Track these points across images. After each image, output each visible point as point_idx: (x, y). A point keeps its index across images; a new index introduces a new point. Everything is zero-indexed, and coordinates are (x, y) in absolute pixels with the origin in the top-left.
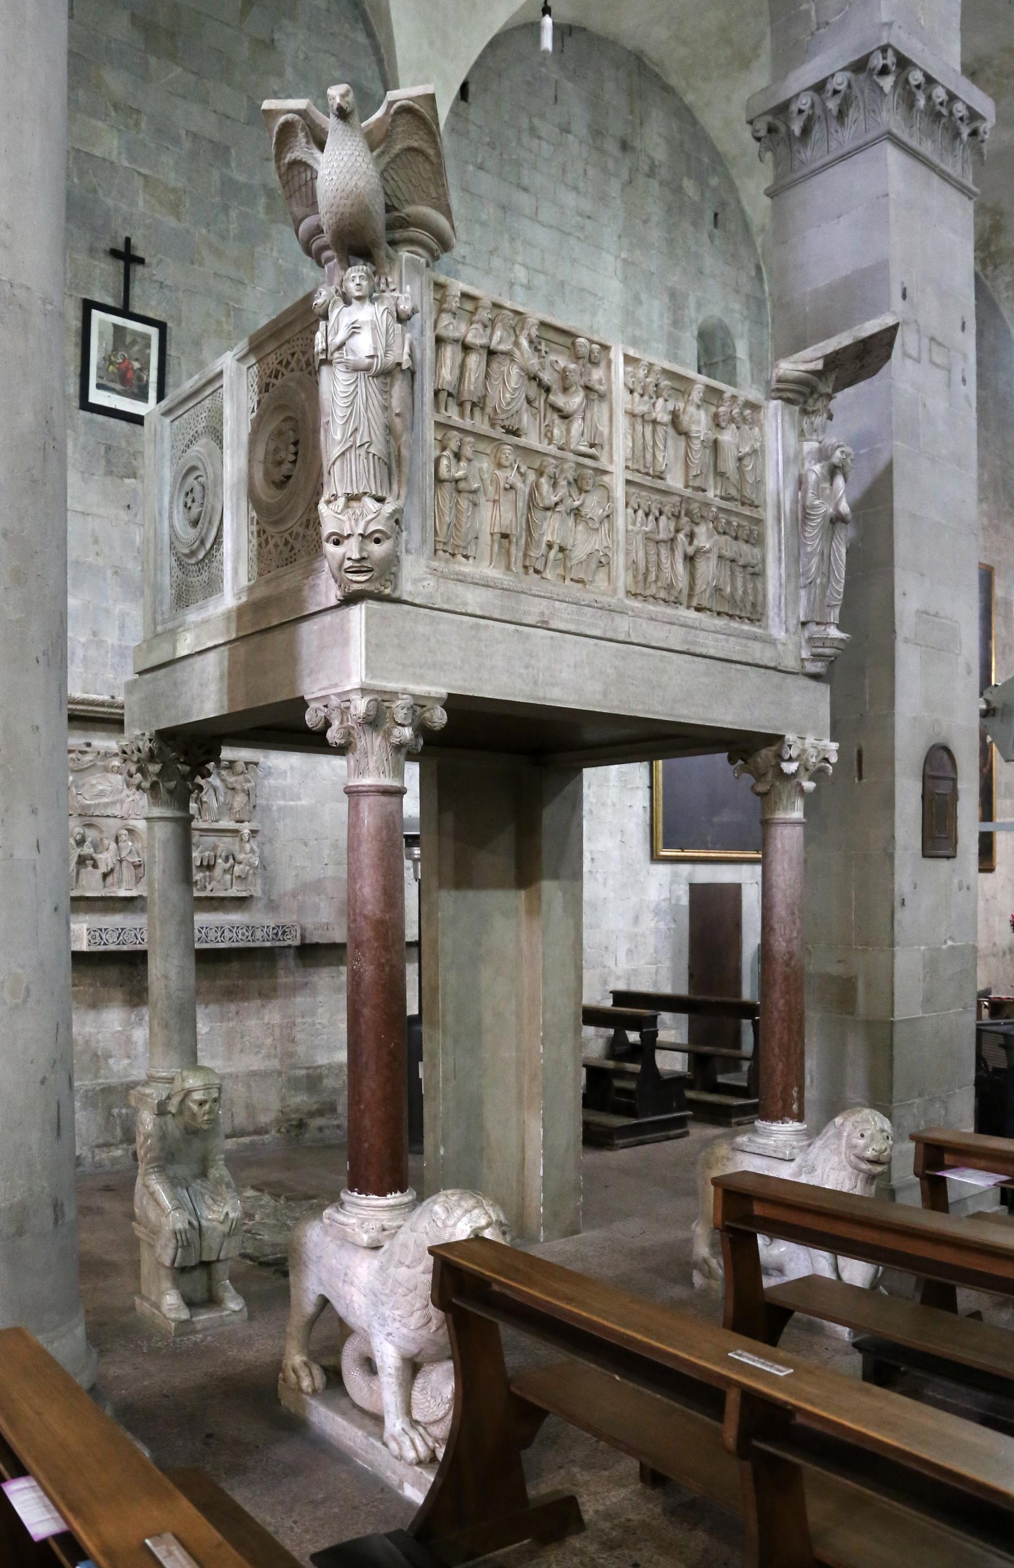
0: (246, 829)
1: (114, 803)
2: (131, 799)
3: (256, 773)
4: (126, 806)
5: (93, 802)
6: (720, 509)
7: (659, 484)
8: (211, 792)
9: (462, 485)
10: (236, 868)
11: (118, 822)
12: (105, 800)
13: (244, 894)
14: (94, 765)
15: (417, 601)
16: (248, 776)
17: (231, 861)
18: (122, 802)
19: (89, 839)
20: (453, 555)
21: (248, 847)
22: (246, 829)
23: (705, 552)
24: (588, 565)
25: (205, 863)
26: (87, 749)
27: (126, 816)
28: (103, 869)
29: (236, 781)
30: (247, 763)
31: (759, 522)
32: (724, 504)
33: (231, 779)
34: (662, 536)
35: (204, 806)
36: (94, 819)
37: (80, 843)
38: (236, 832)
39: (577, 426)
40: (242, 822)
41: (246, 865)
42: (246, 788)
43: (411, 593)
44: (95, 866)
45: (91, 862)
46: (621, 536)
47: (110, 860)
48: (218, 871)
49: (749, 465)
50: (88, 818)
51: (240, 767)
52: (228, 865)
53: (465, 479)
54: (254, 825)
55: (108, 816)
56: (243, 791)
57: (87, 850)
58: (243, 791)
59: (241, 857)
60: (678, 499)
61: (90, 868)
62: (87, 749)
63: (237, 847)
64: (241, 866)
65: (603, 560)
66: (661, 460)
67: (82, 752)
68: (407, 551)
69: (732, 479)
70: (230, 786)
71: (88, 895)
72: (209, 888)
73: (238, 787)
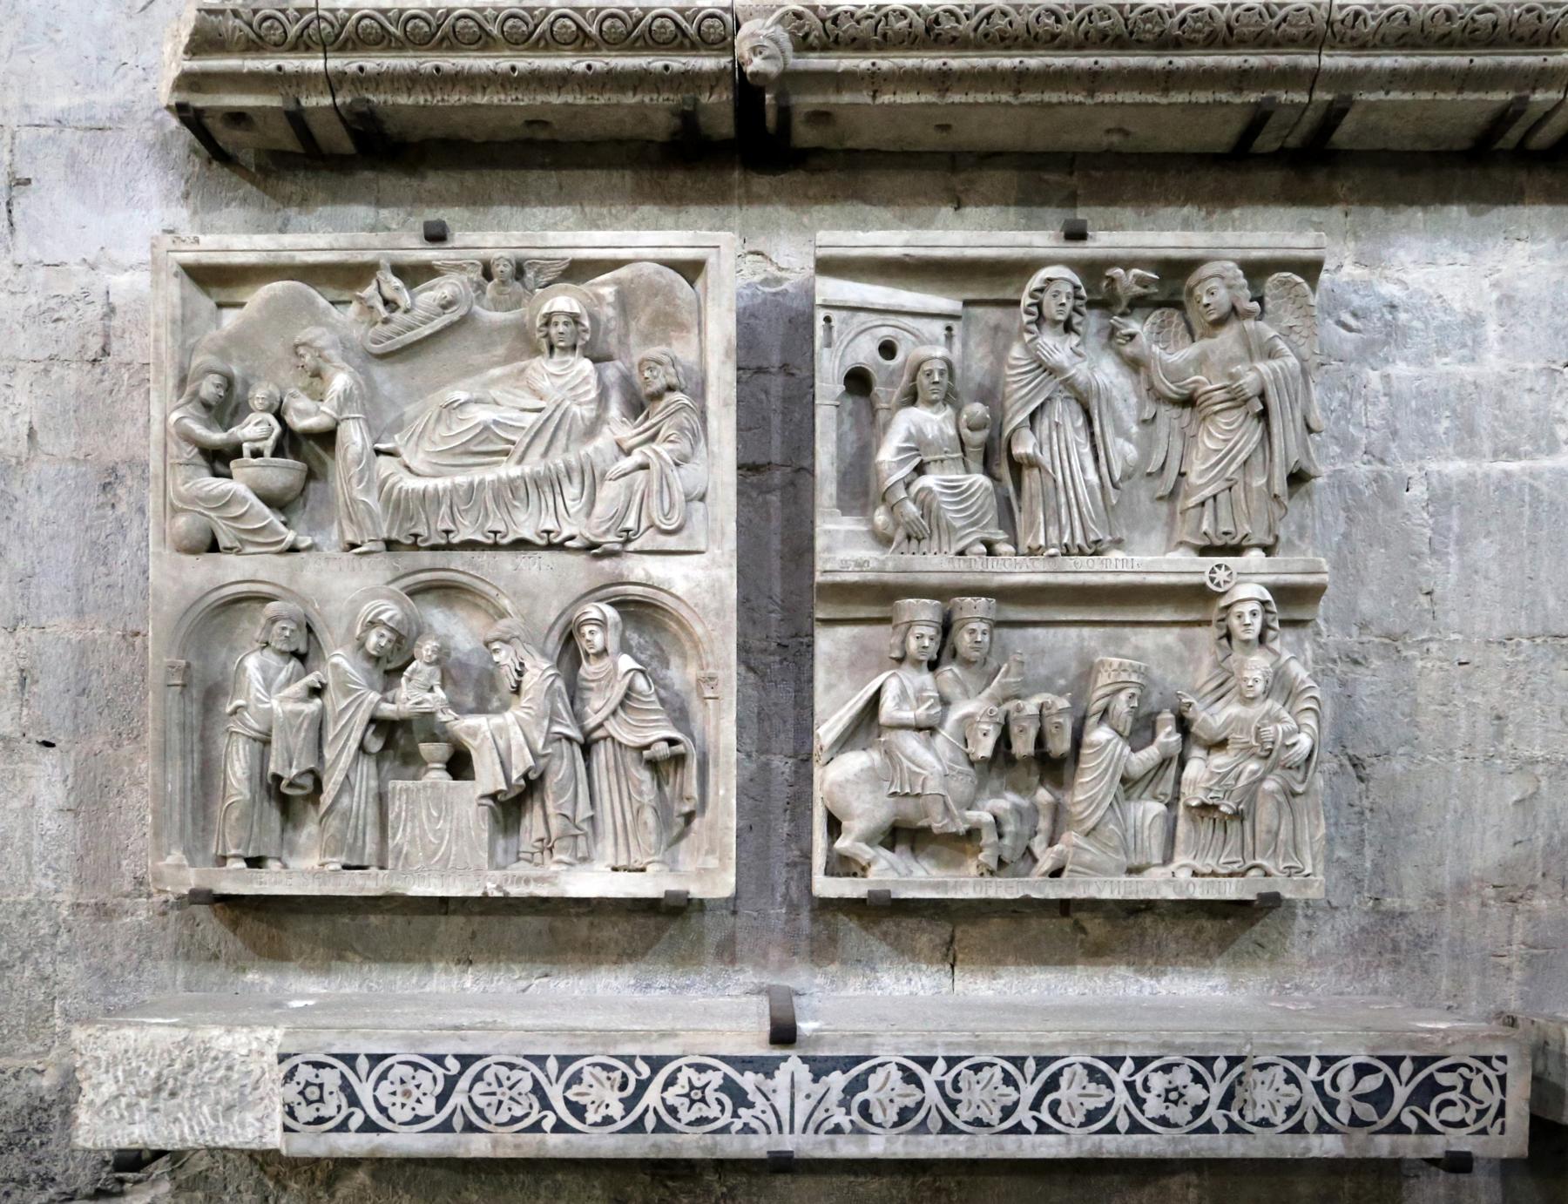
0: (1247, 583)
1: (550, 483)
2: (637, 458)
3: (1305, 310)
4: (609, 493)
5: (442, 483)
8: (1065, 415)
10: (1194, 769)
11: (577, 571)
12: (509, 470)
13: (1230, 890)
14: (464, 321)
16: (1267, 330)
17: (1168, 736)
18: (592, 479)
19: (427, 648)
21: (1256, 667)
22: (1247, 583)
25: (1023, 746)
26: (431, 255)
27: (611, 541)
28: (488, 777)
29: (1201, 361)
30: (1256, 270)
33: (1174, 355)
35: (1031, 479)
36: (458, 560)
37: (390, 666)
38: (1196, 598)
40: (1237, 550)
41: (1248, 752)
42: (1249, 380)
44: (459, 764)
45: (440, 751)
47: (517, 738)
48: (1090, 787)
50: (426, 558)
51: (1218, 287)
52: (1151, 754)
54: (1291, 568)
55: (521, 544)
56: (1237, 399)
57: (414, 695)
58: (1237, 399)
59: (1213, 717)
61: (437, 776)
62: (431, 255)
63: (1204, 673)
64: (1219, 760)
67: (413, 274)
70: (1169, 388)
71: (417, 889)
72: (1046, 862)
73: (1208, 383)
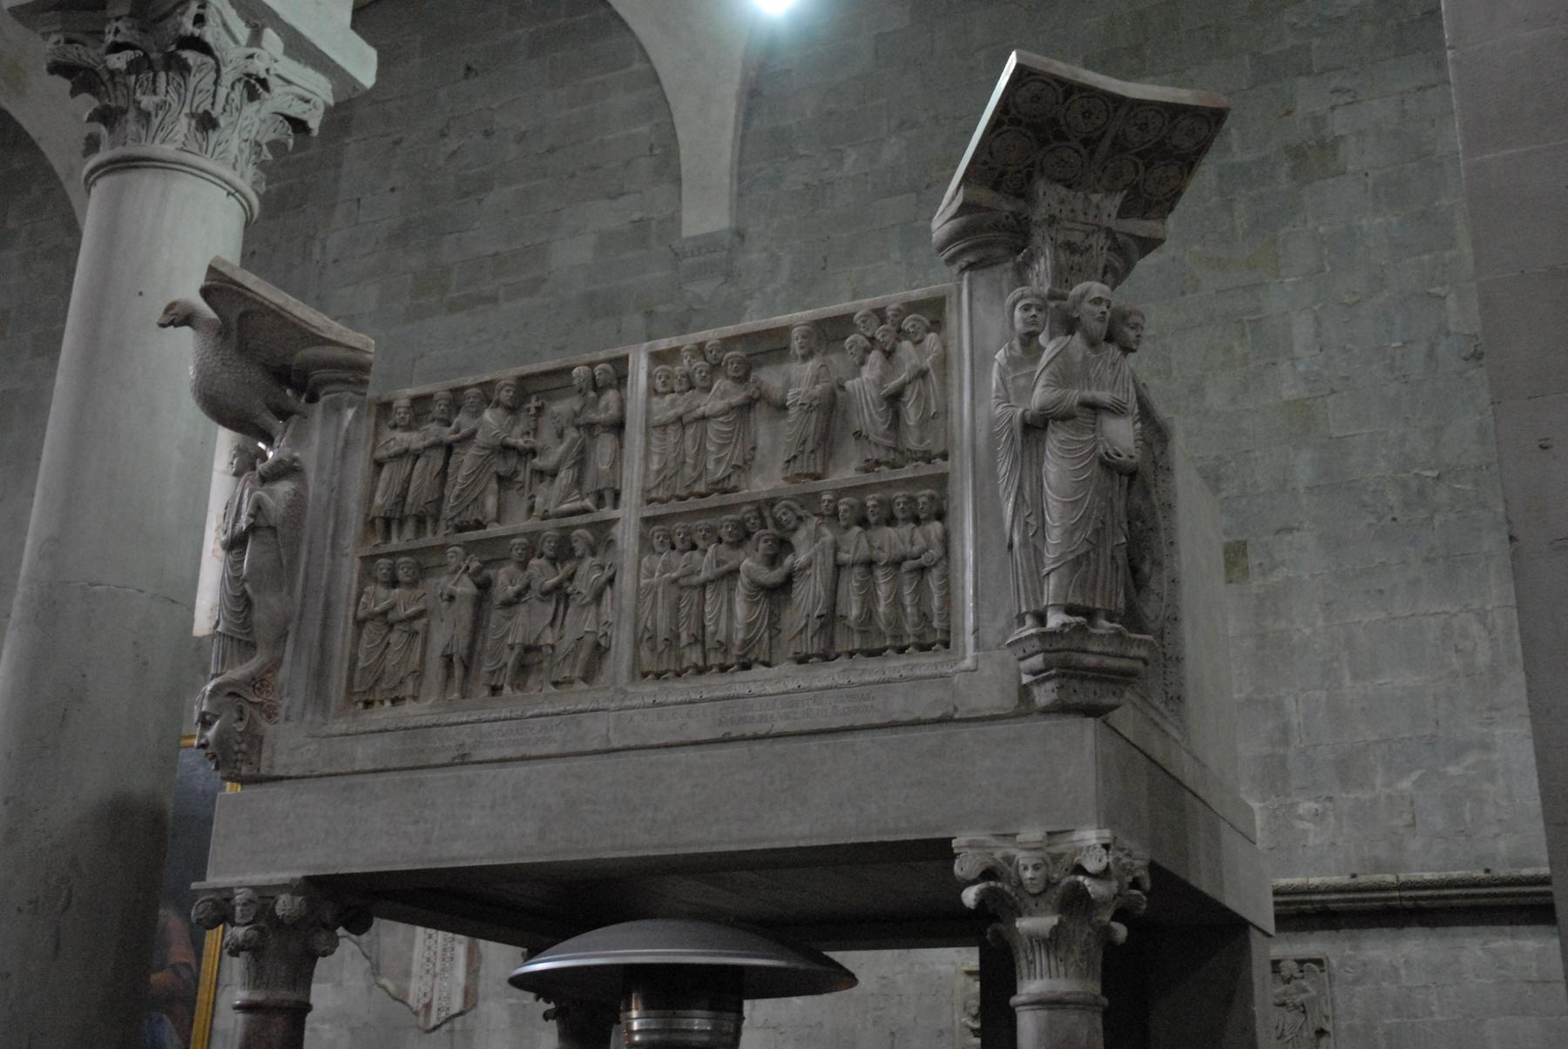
6: (840, 493)
7: (715, 500)
9: (392, 616)
15: (293, 773)
16: (1304, 983)
20: (382, 702)
23: (803, 569)
24: (576, 657)
30: (1301, 962)
31: (942, 480)
32: (872, 478)
34: (703, 576)
39: (565, 476)
42: (1298, 1001)
43: (285, 766)
46: (628, 602)
49: (910, 396)
51: (1289, 967)
53: (393, 607)
58: (1296, 1007)
60: (749, 507)
65: (603, 642)
66: (711, 466)
68: (287, 719)
69: (872, 437)
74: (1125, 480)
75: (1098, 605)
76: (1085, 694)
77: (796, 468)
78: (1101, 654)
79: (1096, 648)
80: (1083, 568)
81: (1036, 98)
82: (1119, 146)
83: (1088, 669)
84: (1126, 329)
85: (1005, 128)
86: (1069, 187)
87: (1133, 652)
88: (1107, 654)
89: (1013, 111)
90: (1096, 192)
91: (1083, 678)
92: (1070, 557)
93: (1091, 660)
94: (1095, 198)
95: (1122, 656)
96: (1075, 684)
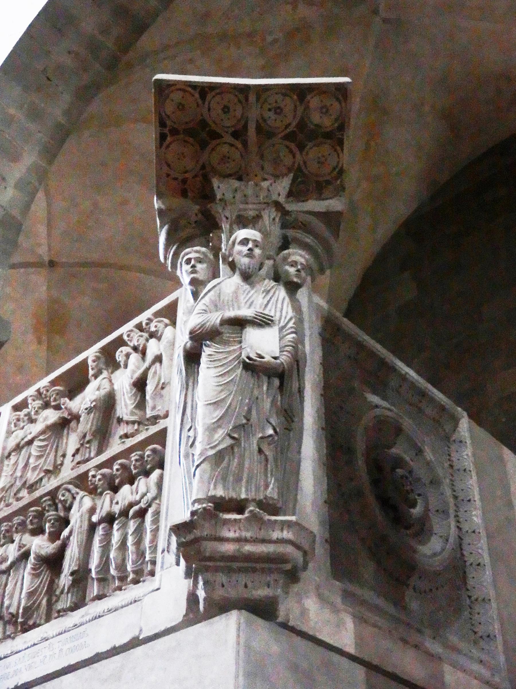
74: (276, 382)
75: (243, 496)
76: (235, 587)
77: (78, 458)
78: (238, 540)
79: (231, 535)
80: (224, 464)
81: (181, 107)
82: (264, 132)
83: (233, 558)
84: (287, 267)
85: (169, 139)
86: (240, 179)
87: (276, 535)
88: (246, 540)
89: (168, 123)
90: (265, 180)
91: (229, 571)
92: (211, 452)
93: (229, 548)
94: (265, 184)
95: (263, 541)
96: (221, 578)
